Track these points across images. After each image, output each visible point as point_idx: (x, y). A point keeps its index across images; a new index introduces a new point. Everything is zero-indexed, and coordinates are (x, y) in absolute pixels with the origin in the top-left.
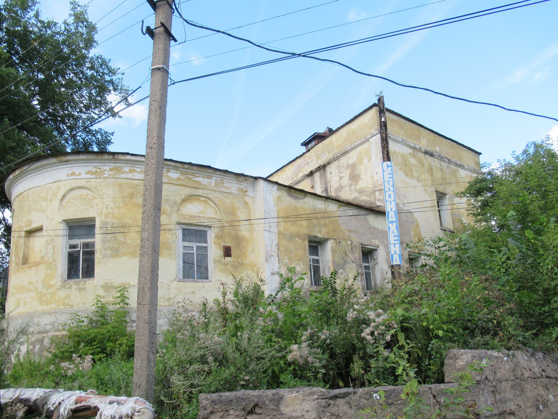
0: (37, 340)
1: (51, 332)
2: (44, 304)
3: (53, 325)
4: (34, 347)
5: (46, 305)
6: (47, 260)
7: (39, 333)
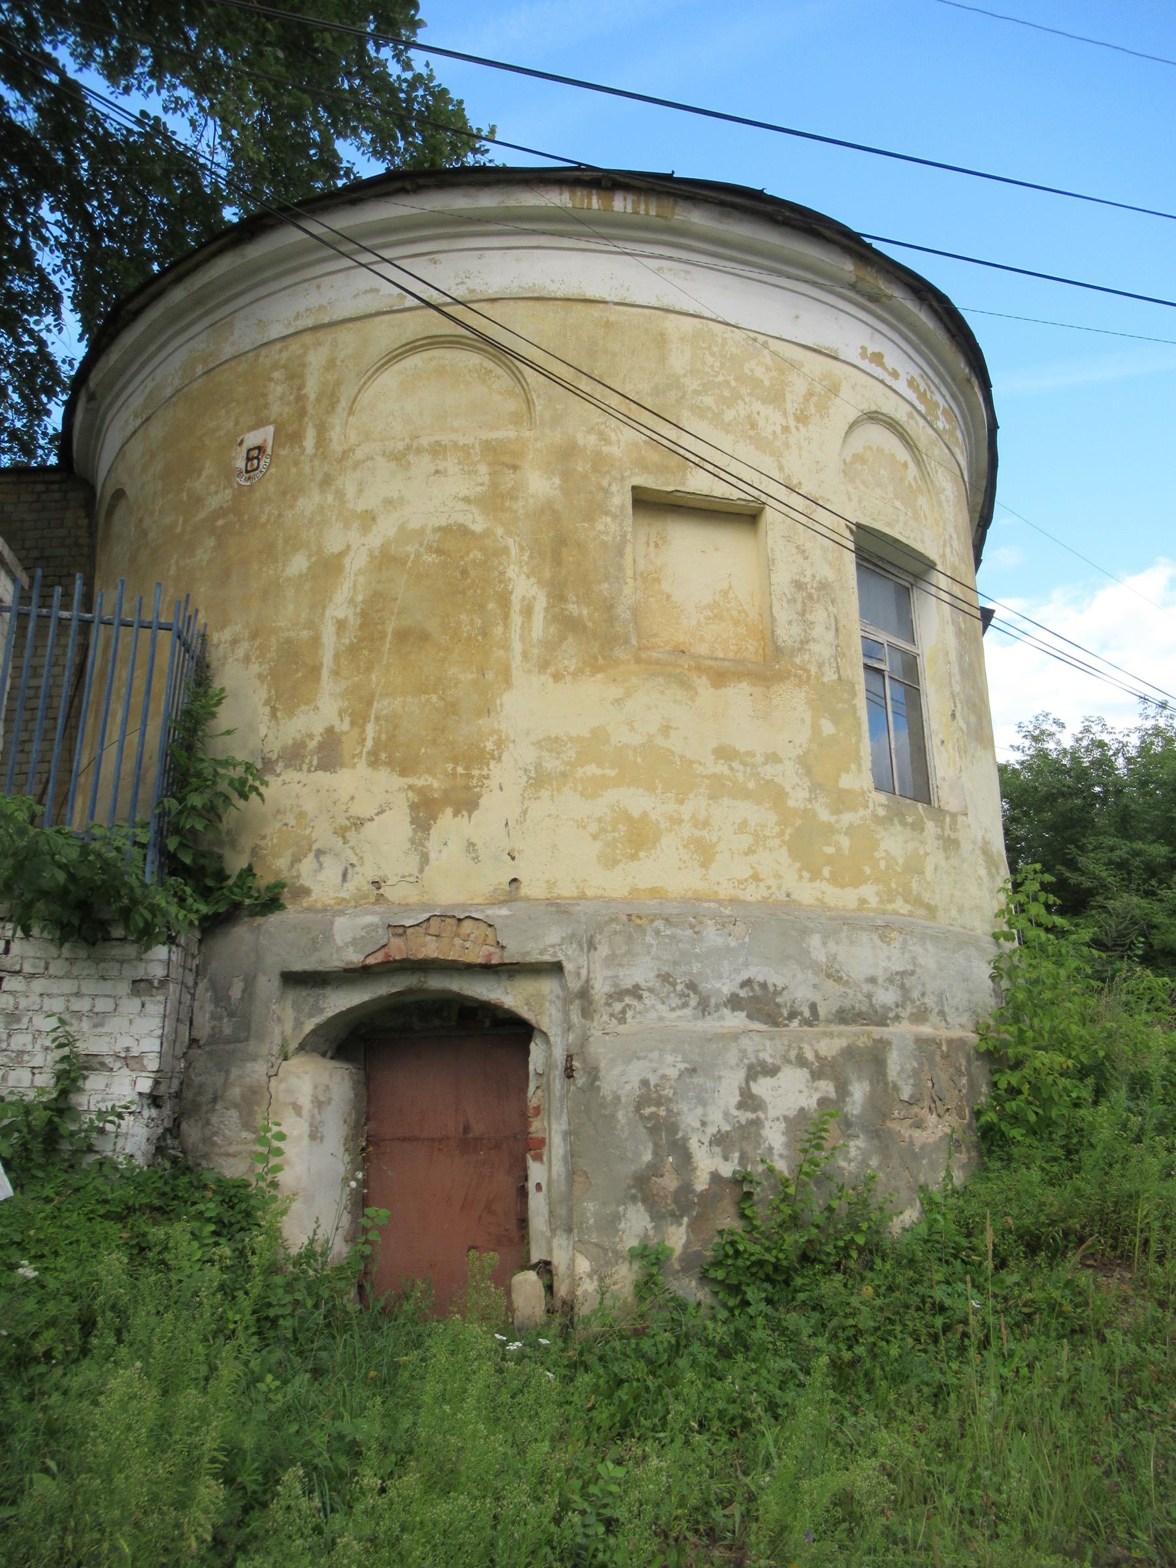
0: (849, 1053)
1: (897, 1018)
2: (826, 871)
3: (903, 987)
4: (843, 1090)
5: (835, 880)
6: (813, 670)
7: (843, 1016)
